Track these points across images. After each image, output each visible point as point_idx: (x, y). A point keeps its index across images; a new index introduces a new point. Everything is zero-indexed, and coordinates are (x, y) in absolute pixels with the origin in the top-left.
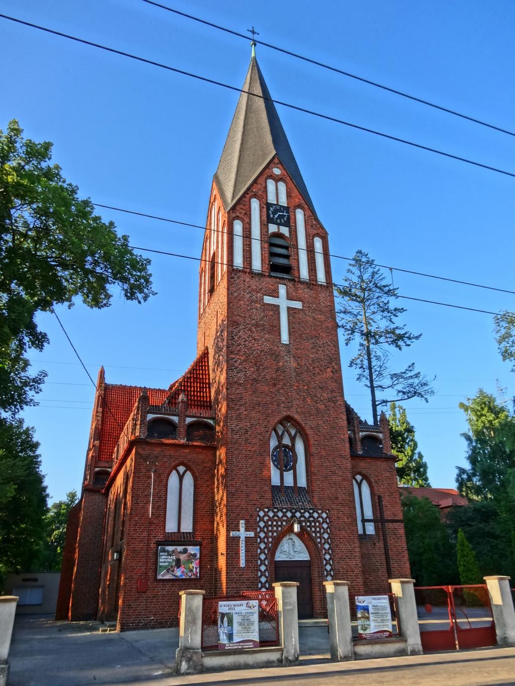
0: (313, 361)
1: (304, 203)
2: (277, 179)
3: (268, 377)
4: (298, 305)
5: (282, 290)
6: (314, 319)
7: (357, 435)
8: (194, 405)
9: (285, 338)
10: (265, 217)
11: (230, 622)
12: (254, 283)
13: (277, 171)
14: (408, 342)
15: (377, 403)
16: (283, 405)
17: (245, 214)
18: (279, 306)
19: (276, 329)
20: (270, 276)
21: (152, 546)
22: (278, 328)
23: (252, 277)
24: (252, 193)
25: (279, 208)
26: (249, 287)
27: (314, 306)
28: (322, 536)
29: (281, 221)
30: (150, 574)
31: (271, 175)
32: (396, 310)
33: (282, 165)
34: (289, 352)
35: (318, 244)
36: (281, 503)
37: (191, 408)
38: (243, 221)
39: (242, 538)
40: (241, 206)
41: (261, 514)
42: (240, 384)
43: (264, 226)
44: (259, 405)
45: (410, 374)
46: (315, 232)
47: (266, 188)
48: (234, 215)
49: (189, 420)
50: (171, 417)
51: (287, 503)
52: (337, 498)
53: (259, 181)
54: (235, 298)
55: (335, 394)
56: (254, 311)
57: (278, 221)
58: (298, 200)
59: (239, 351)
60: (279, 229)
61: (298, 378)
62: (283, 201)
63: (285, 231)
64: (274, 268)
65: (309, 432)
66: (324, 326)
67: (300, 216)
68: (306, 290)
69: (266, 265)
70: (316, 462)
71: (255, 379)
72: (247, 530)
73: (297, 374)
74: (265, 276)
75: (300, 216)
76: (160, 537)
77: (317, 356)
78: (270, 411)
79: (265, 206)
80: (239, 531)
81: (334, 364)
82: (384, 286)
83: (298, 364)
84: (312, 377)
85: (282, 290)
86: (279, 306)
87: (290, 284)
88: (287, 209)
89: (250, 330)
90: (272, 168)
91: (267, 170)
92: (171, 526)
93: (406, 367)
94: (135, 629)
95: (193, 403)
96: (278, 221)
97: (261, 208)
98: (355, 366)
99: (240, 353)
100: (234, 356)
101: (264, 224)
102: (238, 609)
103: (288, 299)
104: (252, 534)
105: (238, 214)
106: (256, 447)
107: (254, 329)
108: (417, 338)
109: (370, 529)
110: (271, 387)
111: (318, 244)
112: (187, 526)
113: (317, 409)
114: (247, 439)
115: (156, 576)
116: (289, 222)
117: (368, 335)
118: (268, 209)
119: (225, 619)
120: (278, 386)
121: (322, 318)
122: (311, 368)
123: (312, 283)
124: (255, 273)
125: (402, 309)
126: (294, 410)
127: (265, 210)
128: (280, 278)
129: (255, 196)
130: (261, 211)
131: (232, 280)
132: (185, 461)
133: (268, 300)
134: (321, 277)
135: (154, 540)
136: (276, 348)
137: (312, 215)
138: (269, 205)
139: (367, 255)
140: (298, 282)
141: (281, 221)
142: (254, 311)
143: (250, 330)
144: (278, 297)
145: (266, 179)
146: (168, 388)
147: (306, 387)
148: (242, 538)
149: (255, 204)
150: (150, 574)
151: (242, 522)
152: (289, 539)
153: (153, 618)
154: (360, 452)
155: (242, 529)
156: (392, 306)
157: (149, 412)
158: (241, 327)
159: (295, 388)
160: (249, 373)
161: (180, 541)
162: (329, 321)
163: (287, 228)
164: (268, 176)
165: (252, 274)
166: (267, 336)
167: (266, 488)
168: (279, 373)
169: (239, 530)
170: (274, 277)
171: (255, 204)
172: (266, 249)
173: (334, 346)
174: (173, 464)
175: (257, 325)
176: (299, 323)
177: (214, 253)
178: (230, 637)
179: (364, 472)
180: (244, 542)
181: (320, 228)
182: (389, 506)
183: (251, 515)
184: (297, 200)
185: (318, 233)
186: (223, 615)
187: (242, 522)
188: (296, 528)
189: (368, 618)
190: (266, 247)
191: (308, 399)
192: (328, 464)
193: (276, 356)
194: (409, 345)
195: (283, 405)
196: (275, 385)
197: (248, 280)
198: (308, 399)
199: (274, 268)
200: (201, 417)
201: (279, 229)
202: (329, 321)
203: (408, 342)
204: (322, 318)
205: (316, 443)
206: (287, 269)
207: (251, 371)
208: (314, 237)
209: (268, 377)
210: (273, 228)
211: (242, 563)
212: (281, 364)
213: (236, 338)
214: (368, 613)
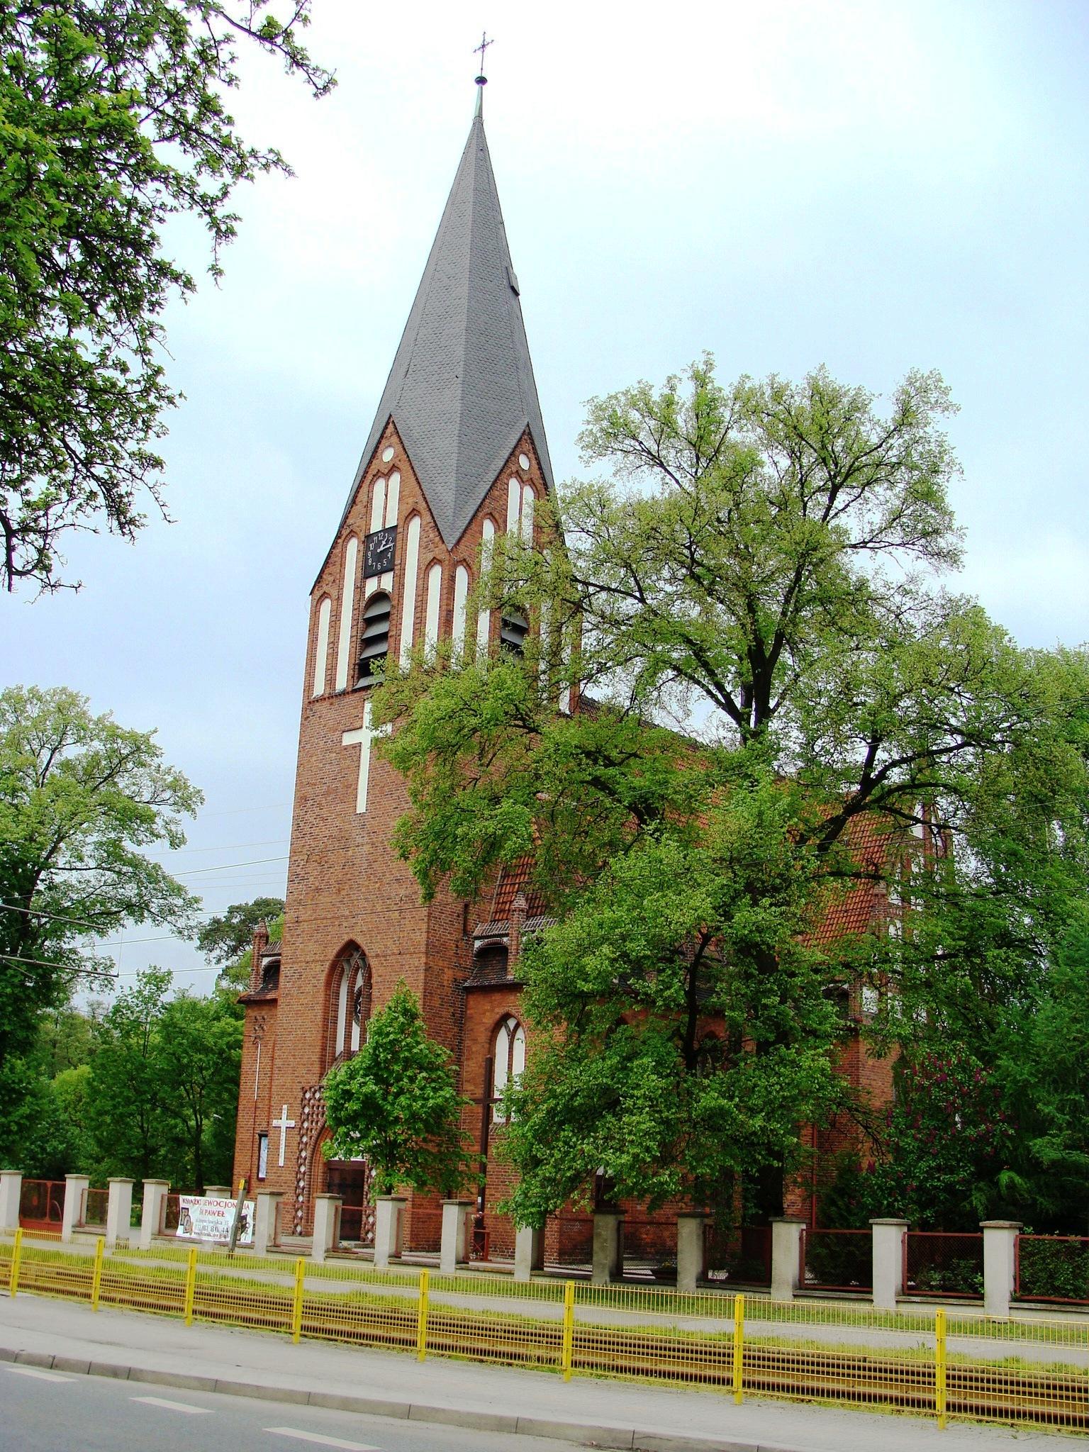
10: (360, 576)
19: (352, 788)
20: (355, 691)
46: (430, 556)
48: (318, 594)
56: (328, 766)
61: (370, 871)
89: (320, 806)
120: (343, 893)
126: (358, 929)
138: (369, 537)
143: (320, 806)
145: (372, 482)
151: (285, 1107)
155: (284, 1116)
171: (353, 547)
175: (327, 793)
187: (285, 1107)
193: (344, 841)
212: (350, 853)
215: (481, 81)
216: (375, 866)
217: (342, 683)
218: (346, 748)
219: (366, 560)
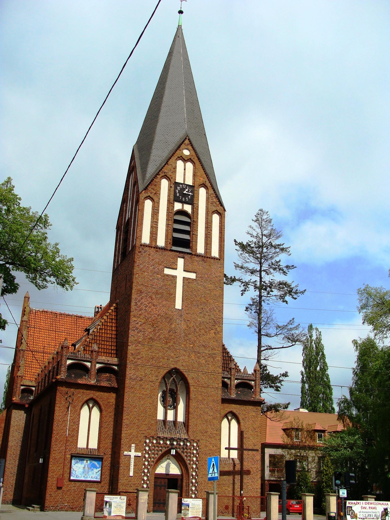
0: (200, 324)
1: (208, 182)
2: (185, 160)
3: (162, 336)
4: (193, 276)
5: (181, 262)
6: (205, 288)
7: (232, 382)
8: (104, 353)
9: (179, 305)
10: (172, 197)
11: (110, 506)
12: (157, 256)
13: (186, 152)
14: (295, 296)
15: (262, 349)
16: (172, 360)
17: (155, 194)
18: (176, 277)
21: (69, 456)
22: (173, 295)
23: (157, 251)
24: (163, 174)
25: (185, 186)
26: (153, 260)
27: (206, 276)
28: (192, 458)
29: (185, 199)
30: (66, 475)
31: (181, 156)
32: (287, 267)
33: (192, 145)
34: (181, 316)
35: (216, 218)
36: (163, 433)
37: (101, 355)
38: (152, 200)
39: (132, 457)
40: (153, 187)
41: (148, 441)
42: (139, 342)
43: (170, 204)
44: (153, 358)
45: (291, 326)
46: (215, 209)
47: (175, 168)
49: (98, 366)
50: (85, 363)
51: (168, 434)
52: (206, 432)
53: (170, 162)
54: (141, 270)
55: (215, 352)
57: (183, 199)
58: (202, 179)
59: (140, 315)
60: (183, 206)
62: (189, 182)
63: (188, 208)
64: (176, 242)
65: (190, 381)
66: (212, 294)
67: (202, 192)
68: (201, 263)
69: (169, 241)
70: (193, 404)
71: (151, 338)
72: (136, 451)
73: (186, 335)
74: (167, 250)
75: (202, 192)
76: (73, 451)
77: (204, 320)
78: (161, 364)
79: (173, 186)
80: (131, 451)
81: (217, 326)
82: (279, 245)
83: (187, 326)
84: (198, 337)
85: (181, 262)
86: (176, 277)
87: (187, 256)
88: (192, 187)
89: (151, 297)
90: (183, 149)
91: (178, 151)
92: (82, 444)
93: (288, 321)
94: (54, 510)
95: (103, 351)
96: (183, 199)
97: (170, 187)
98: (250, 310)
99: (142, 317)
100: (135, 319)
101: (171, 203)
102: (115, 500)
103: (184, 271)
104: (140, 454)
105: (149, 194)
106: (148, 392)
107: (154, 297)
108: (303, 292)
109: (234, 454)
110: (163, 345)
111: (216, 218)
112: (94, 445)
113: (199, 363)
114: (141, 385)
115: (70, 477)
116: (192, 201)
117: (261, 287)
118: (176, 188)
119: (108, 504)
120: (169, 344)
121: (212, 286)
122: (197, 330)
123: (207, 257)
124: (159, 248)
125: (293, 266)
126: (180, 363)
127: (173, 189)
128: (180, 252)
129: (166, 177)
130: (169, 190)
131: (140, 254)
132: (95, 397)
133: (167, 271)
134: (215, 253)
135: (69, 453)
136: (170, 313)
137: (213, 193)
138: (177, 184)
139: (268, 212)
140: (195, 255)
141: (185, 199)
142: (156, 281)
143: (151, 297)
144: (176, 269)
146: (81, 447)
147: (192, 346)
148: (132, 457)
149: (165, 184)
150: (66, 475)
152: (168, 459)
153: (66, 504)
154: (233, 396)
155: (133, 450)
156: (283, 264)
157: (68, 359)
158: (143, 295)
159: (183, 346)
160: (147, 333)
161: (88, 455)
162: (217, 289)
163: (190, 206)
164: (178, 157)
165: (157, 248)
166: (164, 302)
167: (153, 422)
168: (171, 333)
169: (131, 451)
170: (175, 251)
171: (165, 184)
172: (170, 226)
173: (219, 311)
174: (85, 399)
175: (157, 293)
176: (191, 292)
177: (128, 220)
178: (110, 513)
179: (234, 411)
180: (133, 460)
181: (219, 205)
182: (251, 438)
183: (140, 441)
184: (202, 179)
185: (216, 210)
186: (107, 502)
188: (173, 452)
189: (188, 510)
190: (170, 224)
191: (192, 355)
192: (203, 406)
194: (295, 299)
195: (172, 360)
196: (166, 343)
197: (152, 253)
198: (192, 355)
199: (176, 242)
200: (108, 364)
201: (183, 206)
202: (217, 289)
203: (295, 296)
204: (212, 286)
205: (195, 390)
206: (187, 244)
207: (149, 330)
208: (214, 212)
209: (162, 336)
210: (178, 206)
211: (131, 474)
212: (173, 326)
213: (139, 304)
214: (189, 507)
215: (181, 12)
216: (190, 336)
217: (161, 242)
218: (168, 275)
219: (175, 193)
